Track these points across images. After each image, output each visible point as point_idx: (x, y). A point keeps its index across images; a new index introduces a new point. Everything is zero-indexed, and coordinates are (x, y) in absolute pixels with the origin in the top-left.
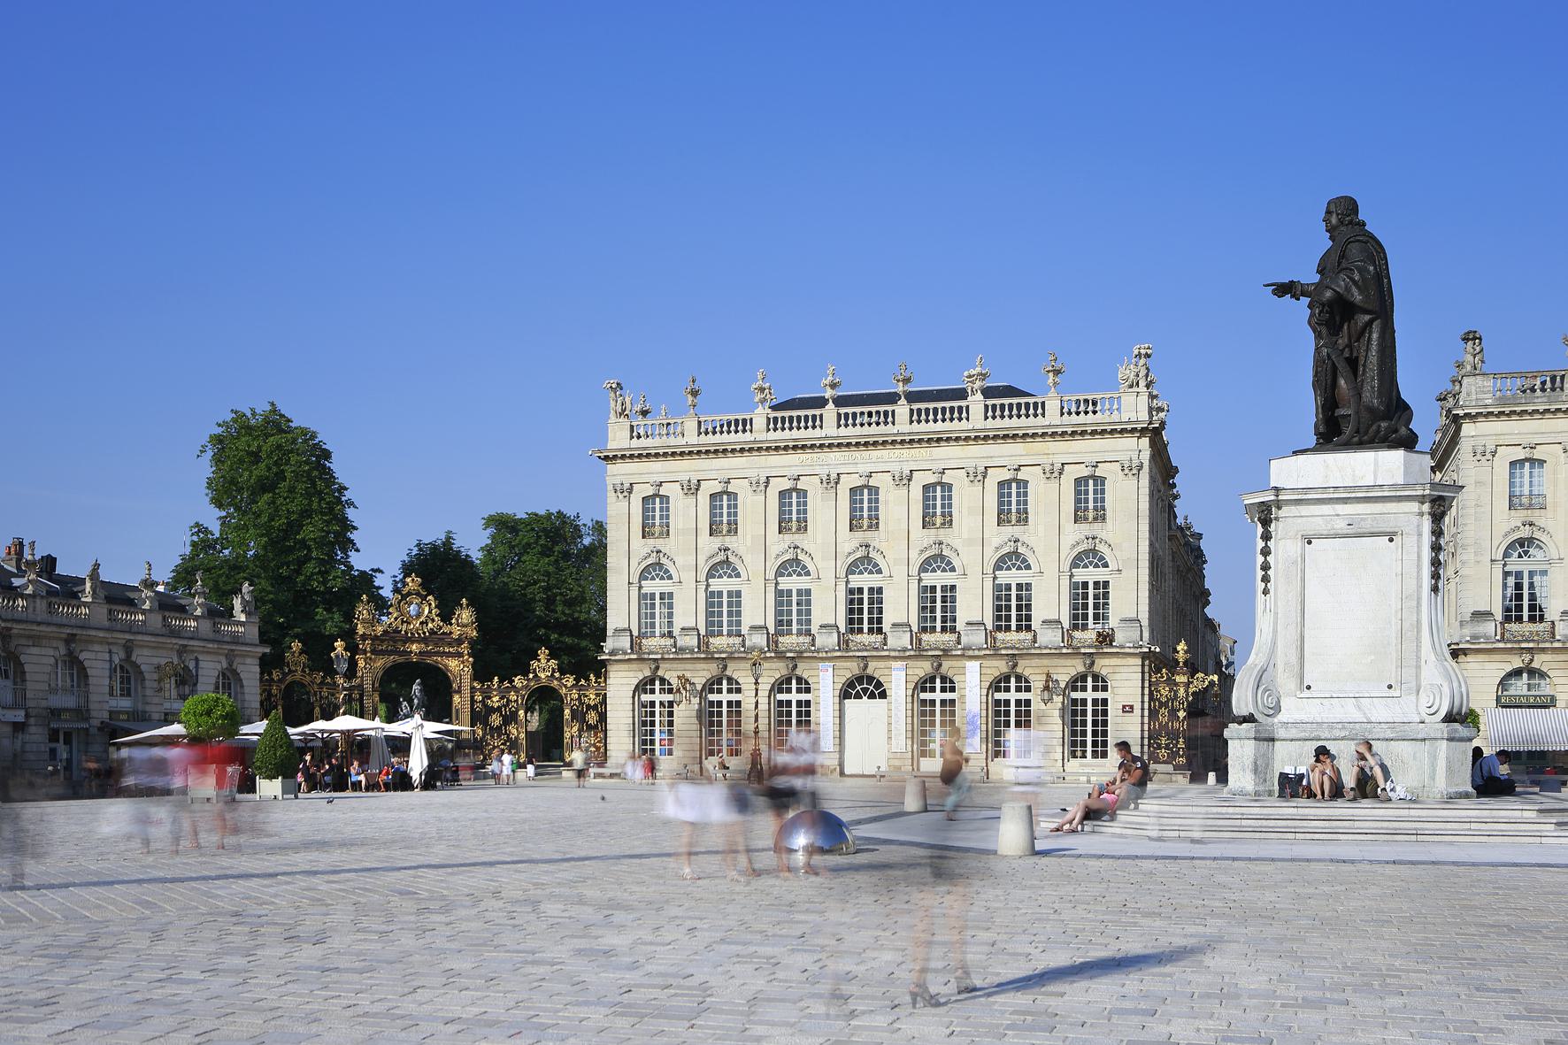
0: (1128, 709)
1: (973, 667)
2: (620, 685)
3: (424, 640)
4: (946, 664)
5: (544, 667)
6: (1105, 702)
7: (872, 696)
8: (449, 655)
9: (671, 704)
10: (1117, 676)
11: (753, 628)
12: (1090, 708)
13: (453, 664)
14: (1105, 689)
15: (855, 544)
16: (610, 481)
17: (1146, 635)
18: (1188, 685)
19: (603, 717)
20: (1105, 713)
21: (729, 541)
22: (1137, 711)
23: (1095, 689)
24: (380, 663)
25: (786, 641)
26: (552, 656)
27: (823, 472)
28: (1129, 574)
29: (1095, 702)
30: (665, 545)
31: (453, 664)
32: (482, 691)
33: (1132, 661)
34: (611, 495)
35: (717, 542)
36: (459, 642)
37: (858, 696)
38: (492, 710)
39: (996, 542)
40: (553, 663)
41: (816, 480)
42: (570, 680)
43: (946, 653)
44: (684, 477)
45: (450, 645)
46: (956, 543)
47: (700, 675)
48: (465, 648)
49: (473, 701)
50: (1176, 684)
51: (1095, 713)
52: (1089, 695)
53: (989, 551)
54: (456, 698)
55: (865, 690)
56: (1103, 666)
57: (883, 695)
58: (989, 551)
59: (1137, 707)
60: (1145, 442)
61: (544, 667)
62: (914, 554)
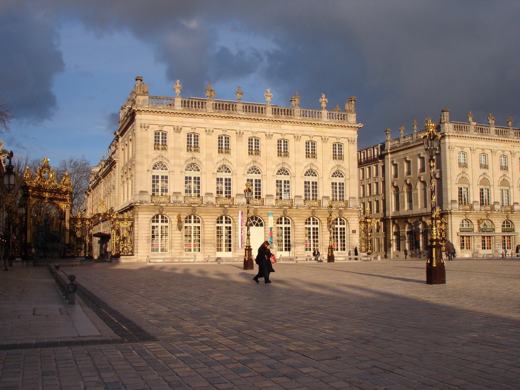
0: (354, 232)
3: (51, 191)
7: (257, 225)
8: (61, 200)
10: (350, 219)
12: (339, 231)
18: (370, 223)
20: (344, 233)
21: (196, 155)
22: (358, 233)
33: (355, 214)
35: (190, 155)
36: (66, 193)
39: (305, 164)
41: (234, 132)
44: (176, 124)
46: (290, 164)
50: (367, 223)
52: (339, 226)
55: (254, 223)
56: (346, 214)
57: (261, 225)
58: (302, 168)
59: (358, 231)
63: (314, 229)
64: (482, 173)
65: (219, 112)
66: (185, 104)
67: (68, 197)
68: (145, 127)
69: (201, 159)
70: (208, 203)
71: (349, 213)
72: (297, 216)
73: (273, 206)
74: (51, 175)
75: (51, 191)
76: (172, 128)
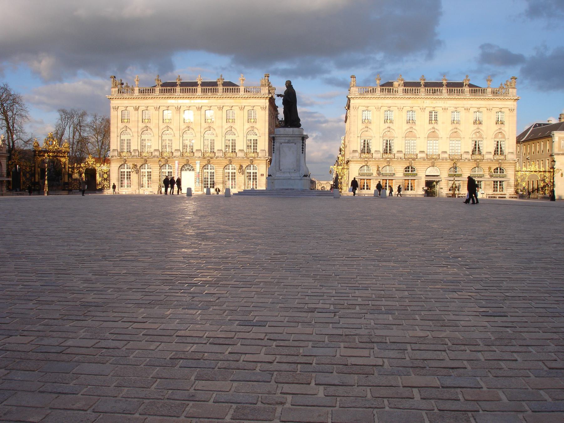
0: (262, 175)
3: (54, 152)
4: (211, 162)
6: (256, 173)
7: (190, 170)
8: (61, 157)
9: (130, 172)
11: (155, 150)
13: (63, 160)
14: (256, 169)
15: (185, 126)
16: (112, 105)
17: (267, 154)
19: (109, 176)
20: (256, 176)
23: (253, 169)
27: (176, 106)
28: (263, 137)
29: (253, 173)
30: (129, 125)
34: (112, 110)
36: (65, 152)
37: (186, 170)
39: (226, 127)
40: (94, 160)
43: (212, 158)
44: (134, 105)
45: (61, 153)
46: (215, 127)
51: (253, 176)
53: (224, 130)
55: (188, 169)
58: (224, 130)
60: (267, 101)
62: (202, 130)
63: (232, 173)
65: (163, 95)
66: (141, 92)
67: (66, 155)
68: (117, 108)
69: (152, 128)
70: (154, 157)
71: (258, 162)
72: (218, 164)
73: (200, 157)
74: (54, 143)
75: (54, 152)
76: (132, 108)
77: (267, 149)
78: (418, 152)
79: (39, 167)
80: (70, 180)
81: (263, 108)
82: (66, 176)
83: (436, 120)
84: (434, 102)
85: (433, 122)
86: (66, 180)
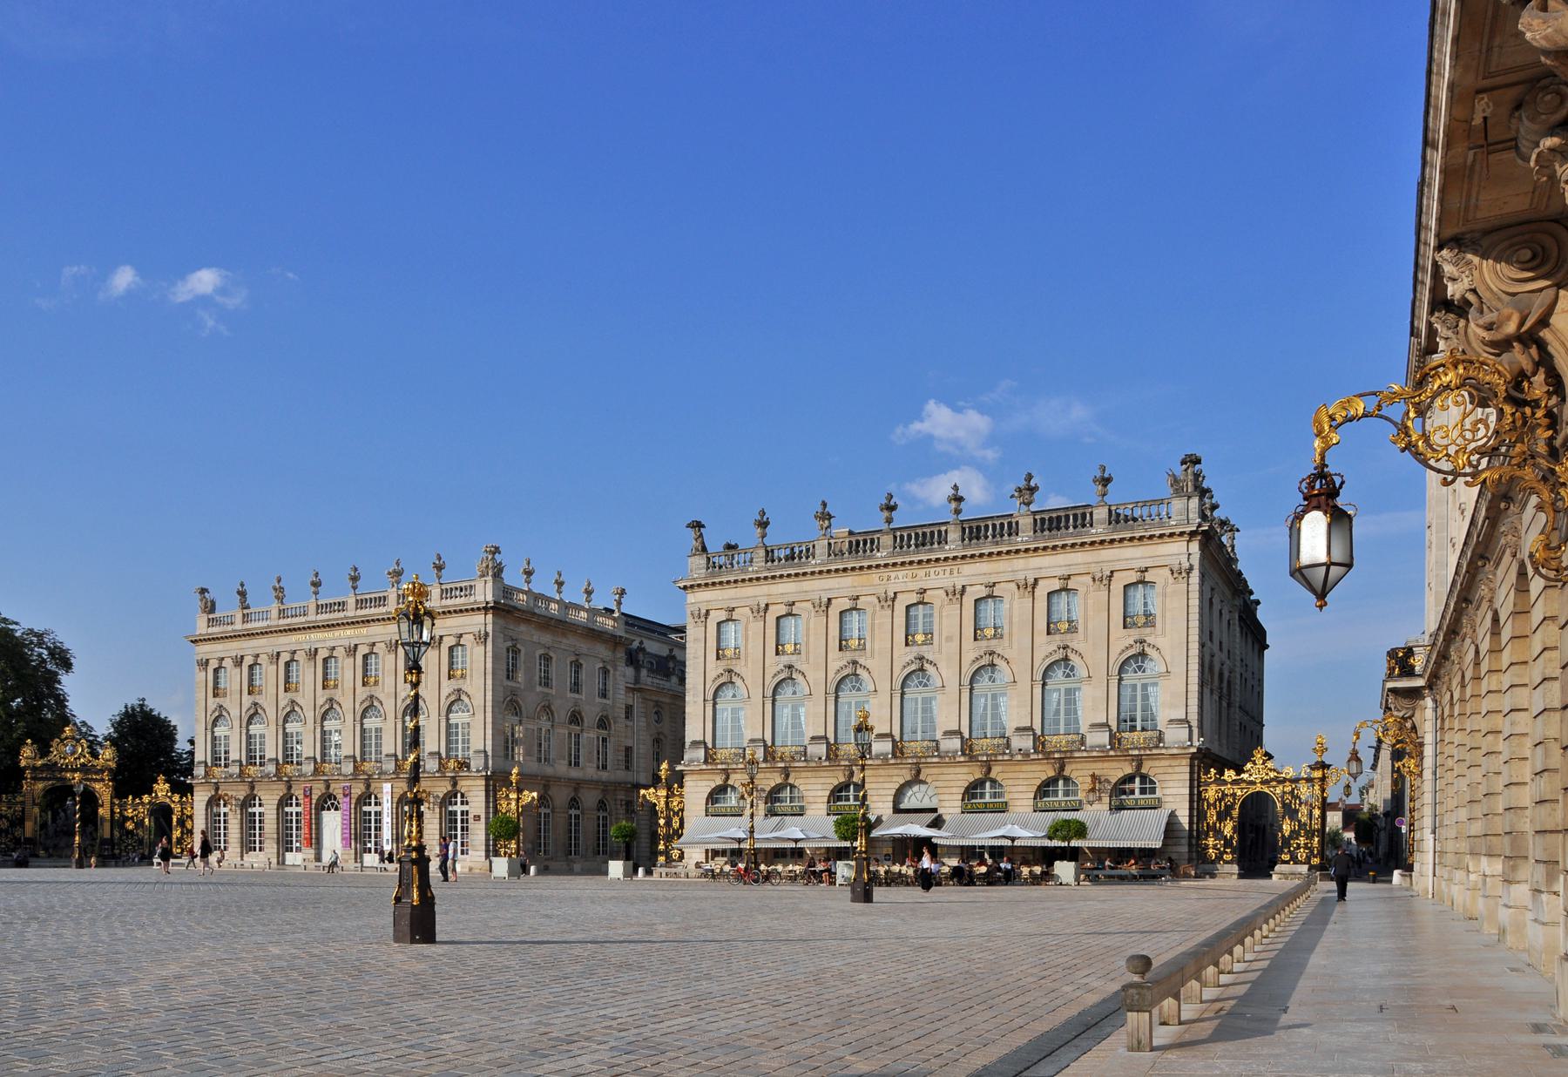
0: (477, 818)
1: (387, 787)
2: (200, 798)
5: (162, 788)
8: (96, 780)
13: (97, 786)
24: (40, 785)
25: (367, 766)
26: (167, 781)
31: (97, 786)
32: (120, 806)
36: (102, 771)
38: (127, 819)
42: (176, 798)
47: (241, 792)
48: (106, 775)
49: (112, 812)
54: (101, 811)
61: (162, 788)
64: (781, 667)
77: (489, 749)
78: (806, 742)
79: (34, 804)
80: (117, 834)
81: (482, 638)
82: (107, 826)
83: (929, 634)
84: (921, 573)
85: (920, 638)
86: (107, 835)
